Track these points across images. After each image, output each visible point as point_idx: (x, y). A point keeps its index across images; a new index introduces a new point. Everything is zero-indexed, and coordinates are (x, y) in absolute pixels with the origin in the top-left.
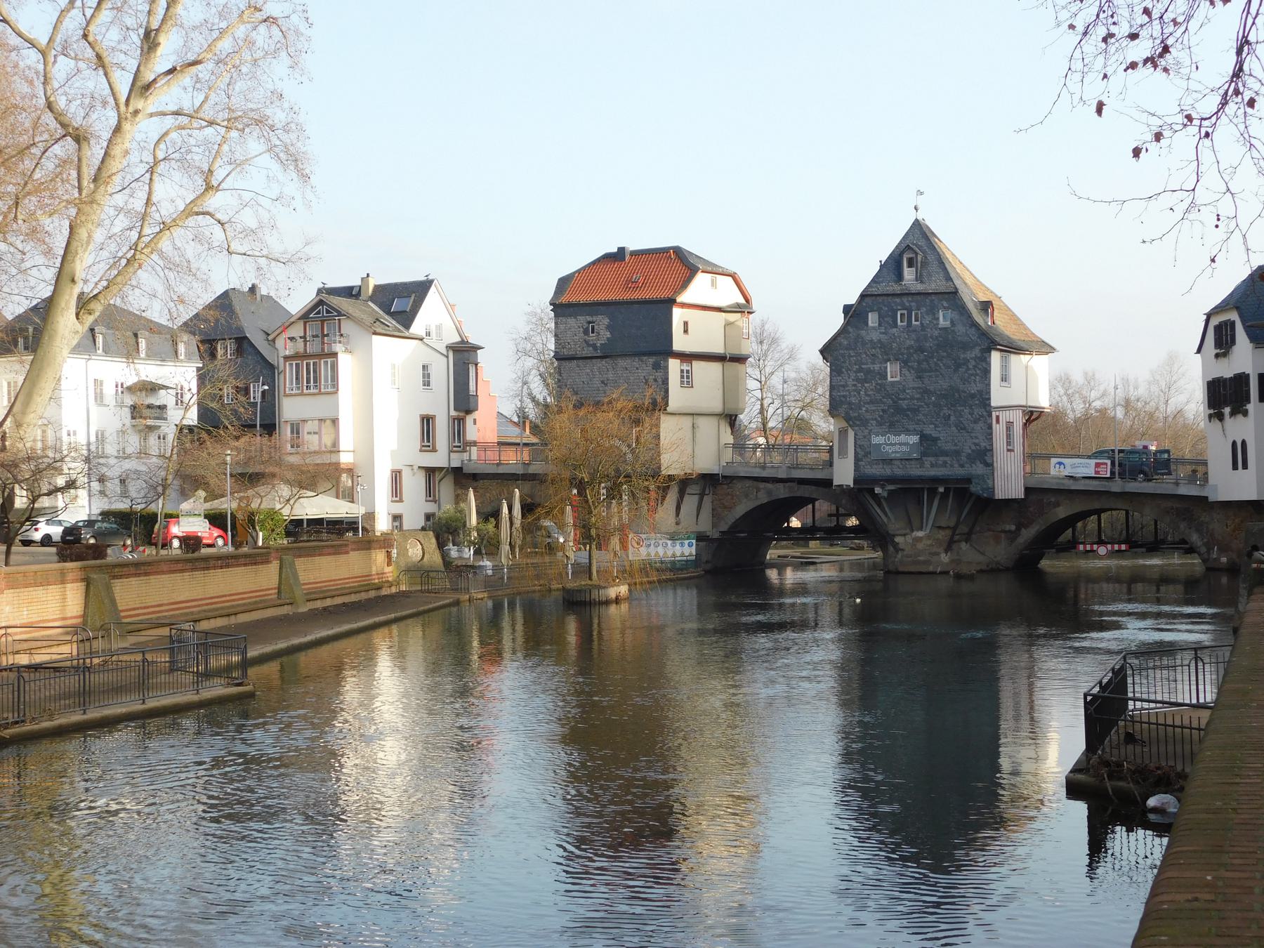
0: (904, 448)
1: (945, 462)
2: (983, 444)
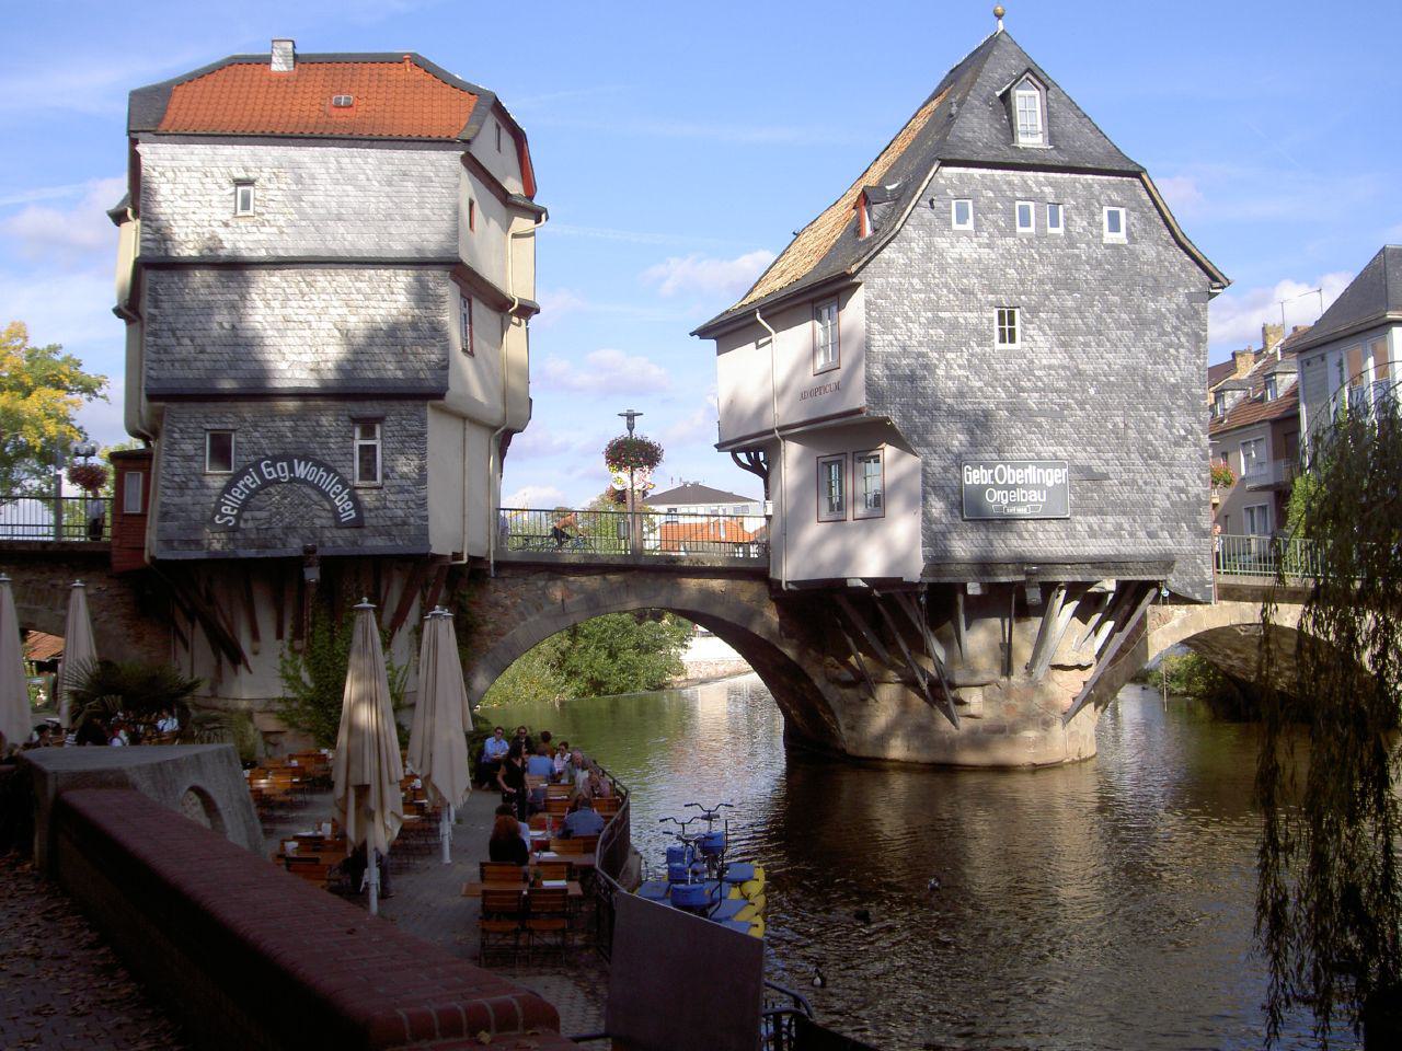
1: (1120, 527)
2: (1193, 490)
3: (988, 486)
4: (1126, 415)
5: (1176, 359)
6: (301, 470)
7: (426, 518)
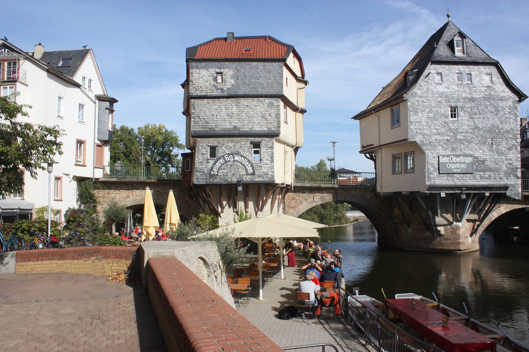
0: (463, 166)
3: (448, 163)
4: (492, 140)
5: (510, 122)
6: (236, 158)
7: (273, 172)
